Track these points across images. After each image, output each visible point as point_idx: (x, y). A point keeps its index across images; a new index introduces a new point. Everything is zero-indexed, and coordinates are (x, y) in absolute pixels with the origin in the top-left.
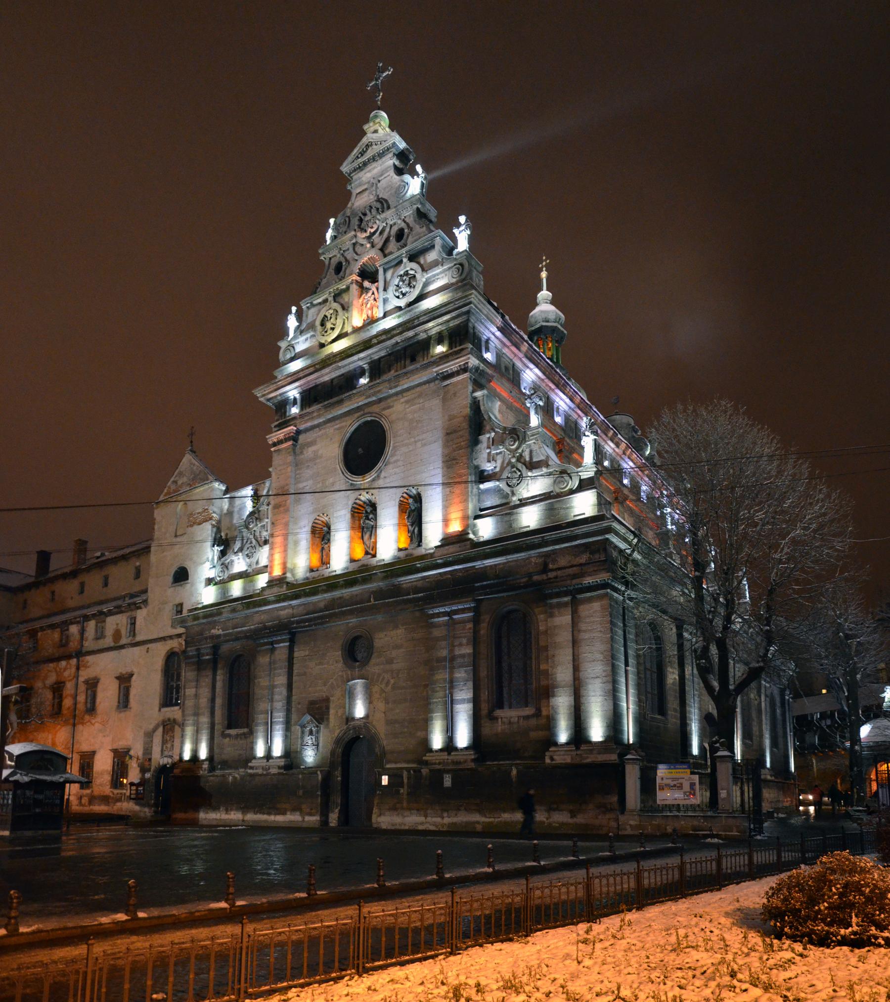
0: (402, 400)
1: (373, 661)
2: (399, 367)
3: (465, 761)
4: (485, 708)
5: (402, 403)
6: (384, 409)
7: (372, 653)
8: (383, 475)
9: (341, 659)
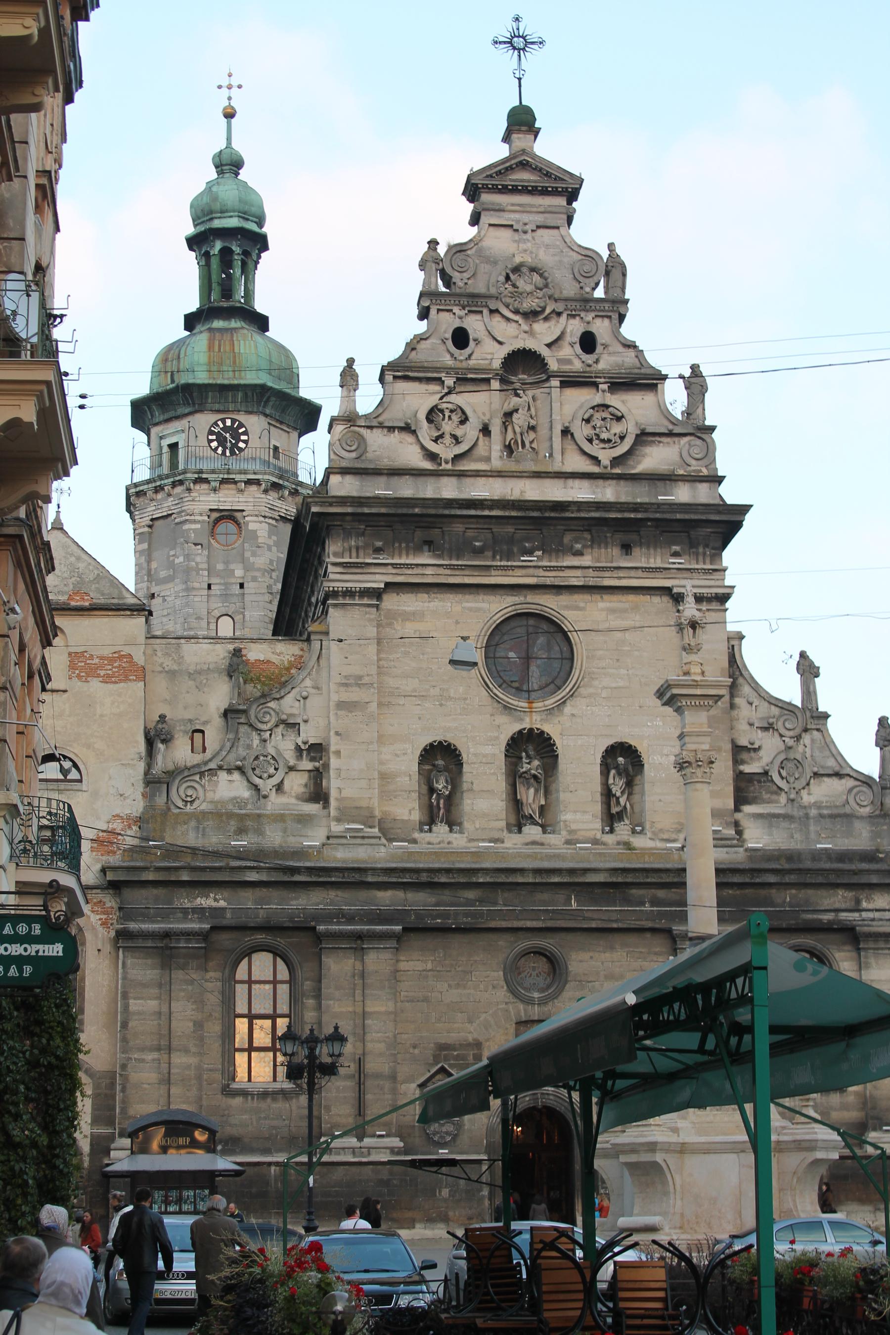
0: (601, 605)
2: (603, 556)
5: (602, 610)
6: (567, 608)
7: (566, 982)
8: (568, 709)
9: (503, 983)
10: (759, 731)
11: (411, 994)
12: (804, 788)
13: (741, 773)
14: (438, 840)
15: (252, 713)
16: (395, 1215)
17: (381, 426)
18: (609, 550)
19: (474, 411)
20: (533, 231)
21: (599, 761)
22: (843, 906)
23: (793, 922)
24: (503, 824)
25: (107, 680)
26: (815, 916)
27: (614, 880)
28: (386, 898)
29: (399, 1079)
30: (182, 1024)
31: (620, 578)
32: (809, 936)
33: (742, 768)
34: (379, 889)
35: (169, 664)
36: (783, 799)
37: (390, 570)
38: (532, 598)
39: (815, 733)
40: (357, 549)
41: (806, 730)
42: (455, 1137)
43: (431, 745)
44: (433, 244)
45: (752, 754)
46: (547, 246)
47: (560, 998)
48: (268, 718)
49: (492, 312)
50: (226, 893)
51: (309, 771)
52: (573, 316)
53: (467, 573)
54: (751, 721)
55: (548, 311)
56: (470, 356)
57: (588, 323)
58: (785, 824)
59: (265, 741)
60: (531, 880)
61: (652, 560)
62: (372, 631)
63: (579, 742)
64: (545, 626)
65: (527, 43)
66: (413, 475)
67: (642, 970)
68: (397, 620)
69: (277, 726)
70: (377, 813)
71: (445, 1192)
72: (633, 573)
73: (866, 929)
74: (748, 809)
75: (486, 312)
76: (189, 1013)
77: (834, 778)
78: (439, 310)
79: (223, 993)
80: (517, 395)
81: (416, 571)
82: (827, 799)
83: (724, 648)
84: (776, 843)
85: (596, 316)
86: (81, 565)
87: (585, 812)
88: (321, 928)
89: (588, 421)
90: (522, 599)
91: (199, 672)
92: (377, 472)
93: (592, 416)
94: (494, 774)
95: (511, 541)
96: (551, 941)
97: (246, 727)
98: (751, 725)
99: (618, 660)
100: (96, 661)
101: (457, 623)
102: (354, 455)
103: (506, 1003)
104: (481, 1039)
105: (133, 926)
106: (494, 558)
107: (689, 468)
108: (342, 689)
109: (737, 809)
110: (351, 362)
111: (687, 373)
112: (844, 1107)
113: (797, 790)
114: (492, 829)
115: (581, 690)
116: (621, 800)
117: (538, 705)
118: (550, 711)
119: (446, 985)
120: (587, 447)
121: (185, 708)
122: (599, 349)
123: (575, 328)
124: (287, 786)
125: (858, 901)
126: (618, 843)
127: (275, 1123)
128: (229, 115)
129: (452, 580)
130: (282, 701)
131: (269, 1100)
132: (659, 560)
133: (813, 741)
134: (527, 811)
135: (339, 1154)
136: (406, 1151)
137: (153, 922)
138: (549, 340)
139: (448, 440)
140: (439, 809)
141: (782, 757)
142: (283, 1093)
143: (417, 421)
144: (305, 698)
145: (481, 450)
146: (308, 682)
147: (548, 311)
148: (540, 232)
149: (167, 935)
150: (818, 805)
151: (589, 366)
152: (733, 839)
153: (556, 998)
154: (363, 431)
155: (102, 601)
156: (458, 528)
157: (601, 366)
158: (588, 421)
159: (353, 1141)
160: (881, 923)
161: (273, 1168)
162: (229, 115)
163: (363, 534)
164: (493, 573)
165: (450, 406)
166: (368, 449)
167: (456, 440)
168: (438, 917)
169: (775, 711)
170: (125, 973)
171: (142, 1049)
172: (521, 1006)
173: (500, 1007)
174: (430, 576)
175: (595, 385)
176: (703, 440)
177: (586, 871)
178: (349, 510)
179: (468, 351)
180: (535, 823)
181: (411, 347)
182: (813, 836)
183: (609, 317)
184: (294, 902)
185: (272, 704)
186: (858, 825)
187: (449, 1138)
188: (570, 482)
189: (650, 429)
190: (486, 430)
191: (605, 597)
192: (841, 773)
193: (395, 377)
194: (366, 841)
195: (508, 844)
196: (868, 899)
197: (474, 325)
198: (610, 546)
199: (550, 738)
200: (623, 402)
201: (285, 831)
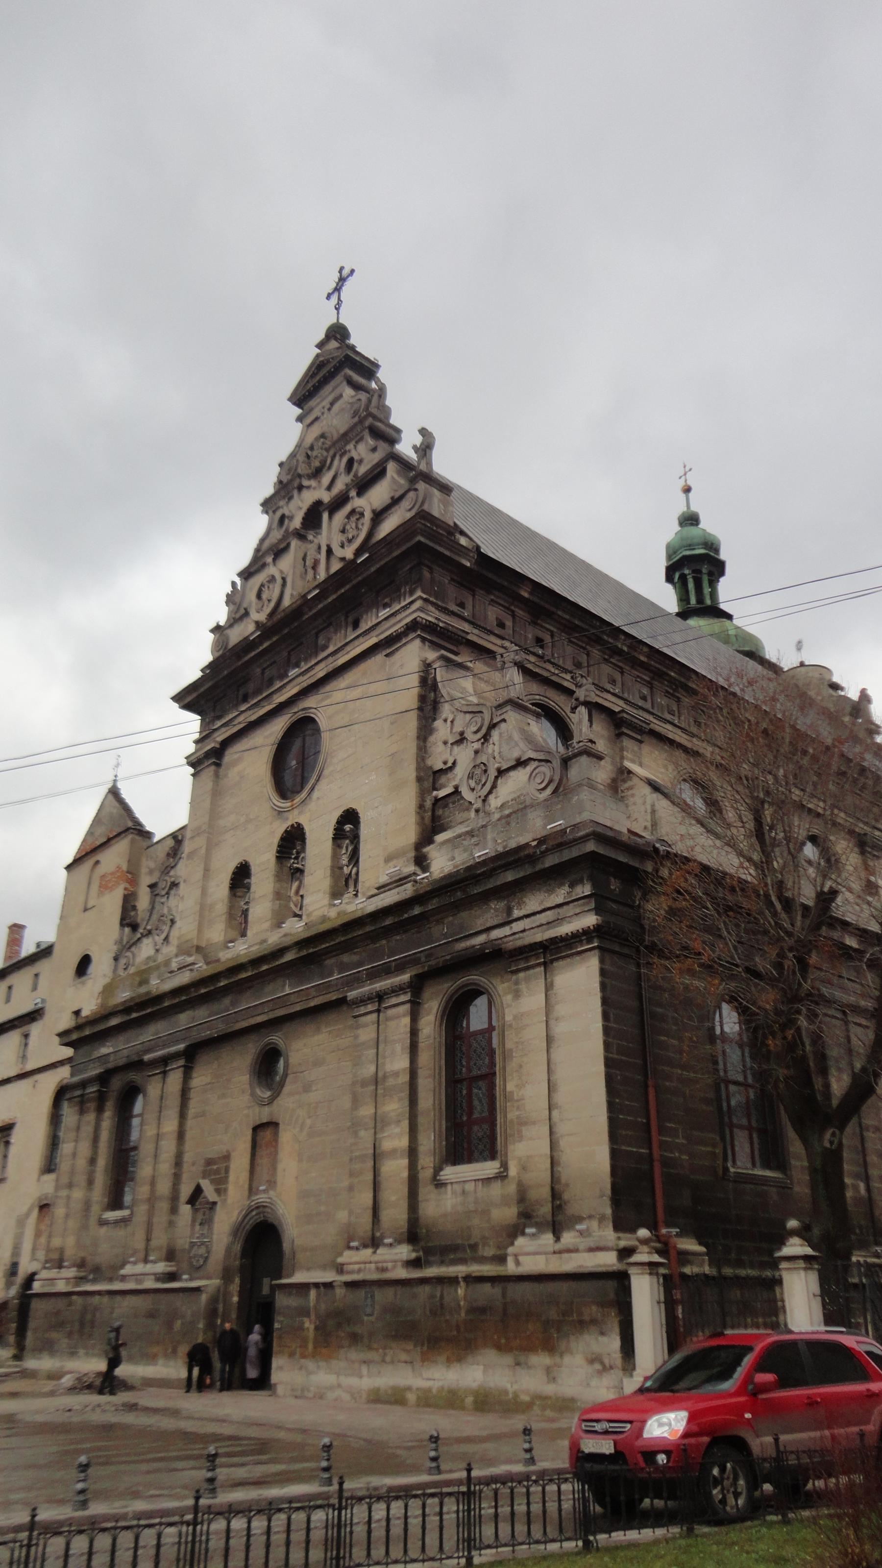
8: (316, 794)
9: (248, 1086)
10: (455, 747)
12: (490, 792)
13: (437, 800)
18: (343, 632)
21: (331, 836)
23: (448, 957)
24: (267, 925)
28: (184, 1019)
31: (348, 652)
32: (475, 972)
33: (435, 793)
34: (181, 1012)
37: (223, 729)
41: (493, 726)
42: (206, 1259)
44: (281, 465)
45: (450, 775)
47: (282, 1095)
49: (300, 488)
62: (210, 785)
67: (339, 1050)
72: (356, 642)
75: (295, 492)
77: (520, 769)
85: (357, 442)
87: (319, 890)
88: (147, 1058)
96: (279, 1034)
98: (445, 743)
100: (110, 877)
112: (505, 1201)
113: (483, 798)
116: (345, 868)
124: (172, 934)
125: (509, 910)
128: (687, 490)
129: (253, 718)
132: (374, 618)
133: (500, 734)
153: (278, 1095)
158: (343, 531)
162: (687, 490)
173: (246, 1112)
176: (416, 490)
181: (257, 550)
189: (379, 509)
192: (522, 760)
196: (520, 905)
199: (303, 829)
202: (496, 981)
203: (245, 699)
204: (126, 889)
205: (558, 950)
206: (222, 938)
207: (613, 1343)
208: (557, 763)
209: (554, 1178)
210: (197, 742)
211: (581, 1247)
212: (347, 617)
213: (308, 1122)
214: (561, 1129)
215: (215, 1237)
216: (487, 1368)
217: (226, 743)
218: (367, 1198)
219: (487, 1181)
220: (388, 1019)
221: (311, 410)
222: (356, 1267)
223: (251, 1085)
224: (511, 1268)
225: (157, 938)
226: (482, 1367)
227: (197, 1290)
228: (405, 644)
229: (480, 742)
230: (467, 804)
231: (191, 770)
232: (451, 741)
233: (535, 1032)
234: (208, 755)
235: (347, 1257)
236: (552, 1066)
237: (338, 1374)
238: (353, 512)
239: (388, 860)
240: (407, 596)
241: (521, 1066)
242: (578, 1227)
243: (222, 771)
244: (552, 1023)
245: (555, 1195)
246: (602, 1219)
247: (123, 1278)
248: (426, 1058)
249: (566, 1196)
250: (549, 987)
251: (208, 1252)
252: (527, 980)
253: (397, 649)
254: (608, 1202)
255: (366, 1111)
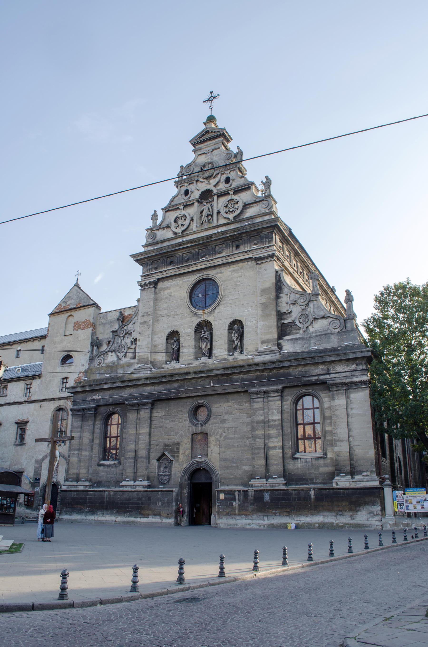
0: (230, 270)
1: (211, 421)
2: (228, 251)
3: (279, 485)
4: (289, 452)
5: (230, 271)
6: (218, 273)
7: (210, 416)
8: (217, 310)
9: (188, 419)
10: (291, 305)
11: (157, 425)
12: (309, 326)
13: (283, 324)
14: (170, 367)
15: (119, 331)
16: (143, 512)
17: (160, 228)
18: (231, 249)
19: (189, 214)
20: (211, 152)
21: (227, 328)
22: (322, 373)
25: (83, 329)
26: (309, 379)
27: (224, 373)
28: (149, 389)
29: (151, 458)
30: (86, 441)
33: (283, 321)
34: (146, 387)
35: (104, 321)
36: (301, 331)
38: (205, 273)
39: (315, 302)
40: (149, 269)
42: (169, 481)
43: (170, 332)
44: (182, 167)
45: (288, 315)
46: (216, 155)
48: (122, 332)
49: (197, 181)
50: (101, 393)
51: (134, 348)
52: (223, 174)
53: (182, 269)
54: (287, 302)
55: (214, 175)
56: (190, 197)
57: (227, 174)
58: (301, 342)
59: (122, 340)
60: (193, 377)
61: (246, 248)
62: (152, 296)
63: (220, 322)
64: (211, 282)
65: (214, 98)
66: (168, 241)
68: (161, 291)
69: (125, 334)
70: (149, 360)
71: (160, 503)
72: (239, 255)
73: (331, 382)
74: (286, 338)
75: (195, 182)
76: (88, 436)
78: (181, 187)
79: (100, 429)
80: (204, 205)
81: (167, 272)
82: (320, 328)
83: (274, 274)
84: (296, 350)
85: (231, 171)
86: (80, 295)
87: (221, 348)
89: (226, 207)
90: (202, 274)
91: (111, 322)
92: (157, 243)
93: (228, 204)
94: (190, 339)
95: (198, 253)
96: (206, 401)
97: (117, 337)
98: (287, 303)
99: (235, 289)
101: (181, 287)
102: (152, 240)
103: (189, 427)
104: (179, 441)
105: (76, 407)
106: (192, 262)
107: (262, 212)
108: (142, 318)
109: (280, 337)
110: (155, 211)
111: (264, 180)
114: (188, 360)
115: (222, 303)
117: (206, 311)
118: (210, 312)
119: (169, 421)
120: (226, 216)
121: (107, 334)
122: (231, 181)
123: (224, 177)
125: (329, 370)
126: (233, 359)
127: (112, 476)
130: (128, 326)
131: (111, 467)
132: (249, 247)
133: (314, 305)
134: (203, 351)
135: (126, 487)
136: (149, 486)
137: (81, 406)
138: (214, 184)
139: (180, 226)
140: (173, 355)
141: (301, 314)
142: (114, 464)
143: (171, 223)
144: (134, 323)
145: (191, 227)
146: (136, 318)
147: (214, 175)
148: (214, 151)
149: (83, 410)
150: (316, 332)
151: (227, 188)
152: (276, 350)
153: (206, 423)
154: (156, 232)
155: (84, 304)
156: (180, 254)
157: (232, 186)
159: (132, 483)
160: (339, 378)
161: (106, 493)
163: (152, 264)
164: (191, 267)
165: (181, 215)
166: (157, 237)
167: (183, 225)
168: (165, 395)
169: (298, 296)
170: (72, 424)
171: (74, 450)
172: (194, 428)
173: (187, 428)
174: (171, 273)
175: (228, 194)
177: (213, 370)
178: (144, 257)
179: (188, 196)
180: (206, 356)
181: (172, 201)
182: (312, 345)
183: (235, 170)
184: (121, 394)
185: (125, 328)
186: (332, 337)
187: (166, 482)
188: (219, 228)
189: (247, 203)
190: (192, 220)
191: (231, 266)
193: (166, 212)
194: (146, 370)
195: (194, 365)
196: (334, 368)
197: (192, 188)
198: (231, 247)
200: (239, 197)
201: (124, 370)
202: (320, 393)
203: (171, 263)
204: (92, 330)
205: (351, 386)
206: (164, 359)
207: (379, 508)
208: (342, 321)
209: (351, 459)
210: (142, 276)
211: (365, 480)
212: (232, 243)
213: (224, 434)
214: (352, 444)
215: (173, 473)
216: (324, 516)
217: (159, 280)
218: (262, 462)
219: (318, 459)
220: (269, 401)
221: (201, 149)
222: (259, 485)
223: (189, 418)
224: (334, 485)
225: (118, 354)
226: (322, 516)
227: (172, 491)
228: (267, 262)
229: (304, 306)
230: (298, 327)
231: (140, 288)
232: (289, 303)
233: (342, 412)
234: (150, 283)
235: (252, 482)
236: (349, 424)
237: (252, 520)
238: (232, 200)
239: (263, 342)
240: (267, 243)
241: (335, 423)
242: (363, 474)
243: (157, 290)
244: (349, 410)
245: (351, 464)
246: (372, 472)
247: (122, 486)
248: (285, 416)
249: (355, 465)
250: (347, 398)
251: (170, 478)
252: (338, 394)
253: (263, 263)
254: (374, 467)
255: (260, 432)
